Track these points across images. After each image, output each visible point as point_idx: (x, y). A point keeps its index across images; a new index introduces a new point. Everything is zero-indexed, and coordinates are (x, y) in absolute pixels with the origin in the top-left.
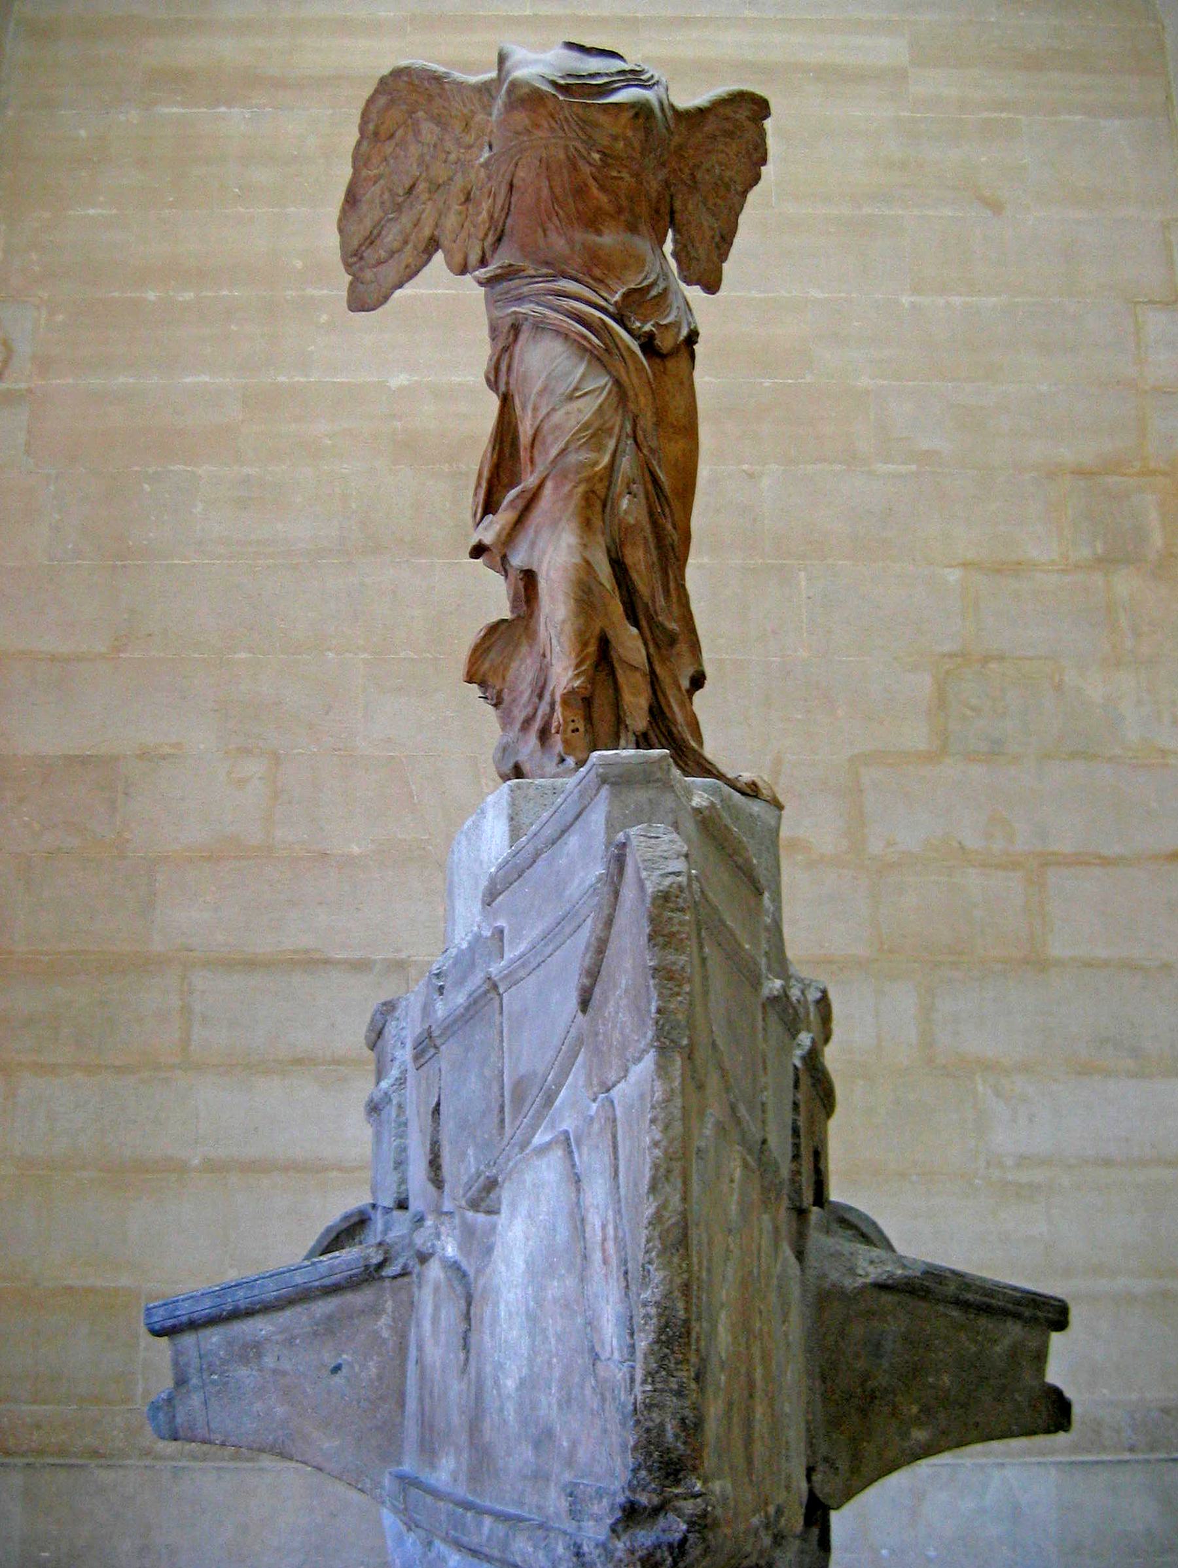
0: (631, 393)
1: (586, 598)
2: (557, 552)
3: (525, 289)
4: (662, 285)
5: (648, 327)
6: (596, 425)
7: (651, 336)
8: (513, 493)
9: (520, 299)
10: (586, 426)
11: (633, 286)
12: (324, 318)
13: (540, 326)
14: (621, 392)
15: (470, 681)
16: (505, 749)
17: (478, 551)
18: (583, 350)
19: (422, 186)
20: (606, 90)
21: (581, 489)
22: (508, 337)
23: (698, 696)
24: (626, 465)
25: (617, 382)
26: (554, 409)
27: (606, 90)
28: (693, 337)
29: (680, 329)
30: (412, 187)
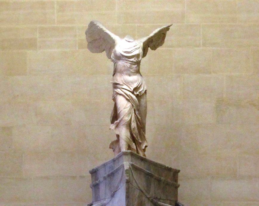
0: (134, 105)
3: (118, 87)
4: (140, 84)
5: (138, 93)
6: (128, 113)
7: (138, 95)
8: (116, 122)
10: (127, 113)
11: (135, 86)
13: (121, 95)
15: (110, 148)
18: (127, 99)
21: (126, 124)
25: (132, 104)
26: (122, 110)
28: (146, 92)
29: (143, 91)
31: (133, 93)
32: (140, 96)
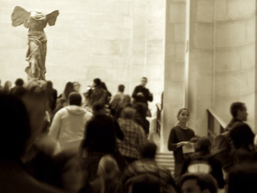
1: (35, 65)
2: (33, 61)
9: (31, 38)
12: (4, 12)
13: (33, 41)
14: (39, 48)
16: (28, 77)
17: (26, 60)
19: (21, 17)
20: (39, 18)
22: (30, 41)
23: (46, 74)
24: (39, 54)
27: (39, 18)
28: (46, 41)
30: (20, 16)
31: (40, 40)
32: (44, 43)
